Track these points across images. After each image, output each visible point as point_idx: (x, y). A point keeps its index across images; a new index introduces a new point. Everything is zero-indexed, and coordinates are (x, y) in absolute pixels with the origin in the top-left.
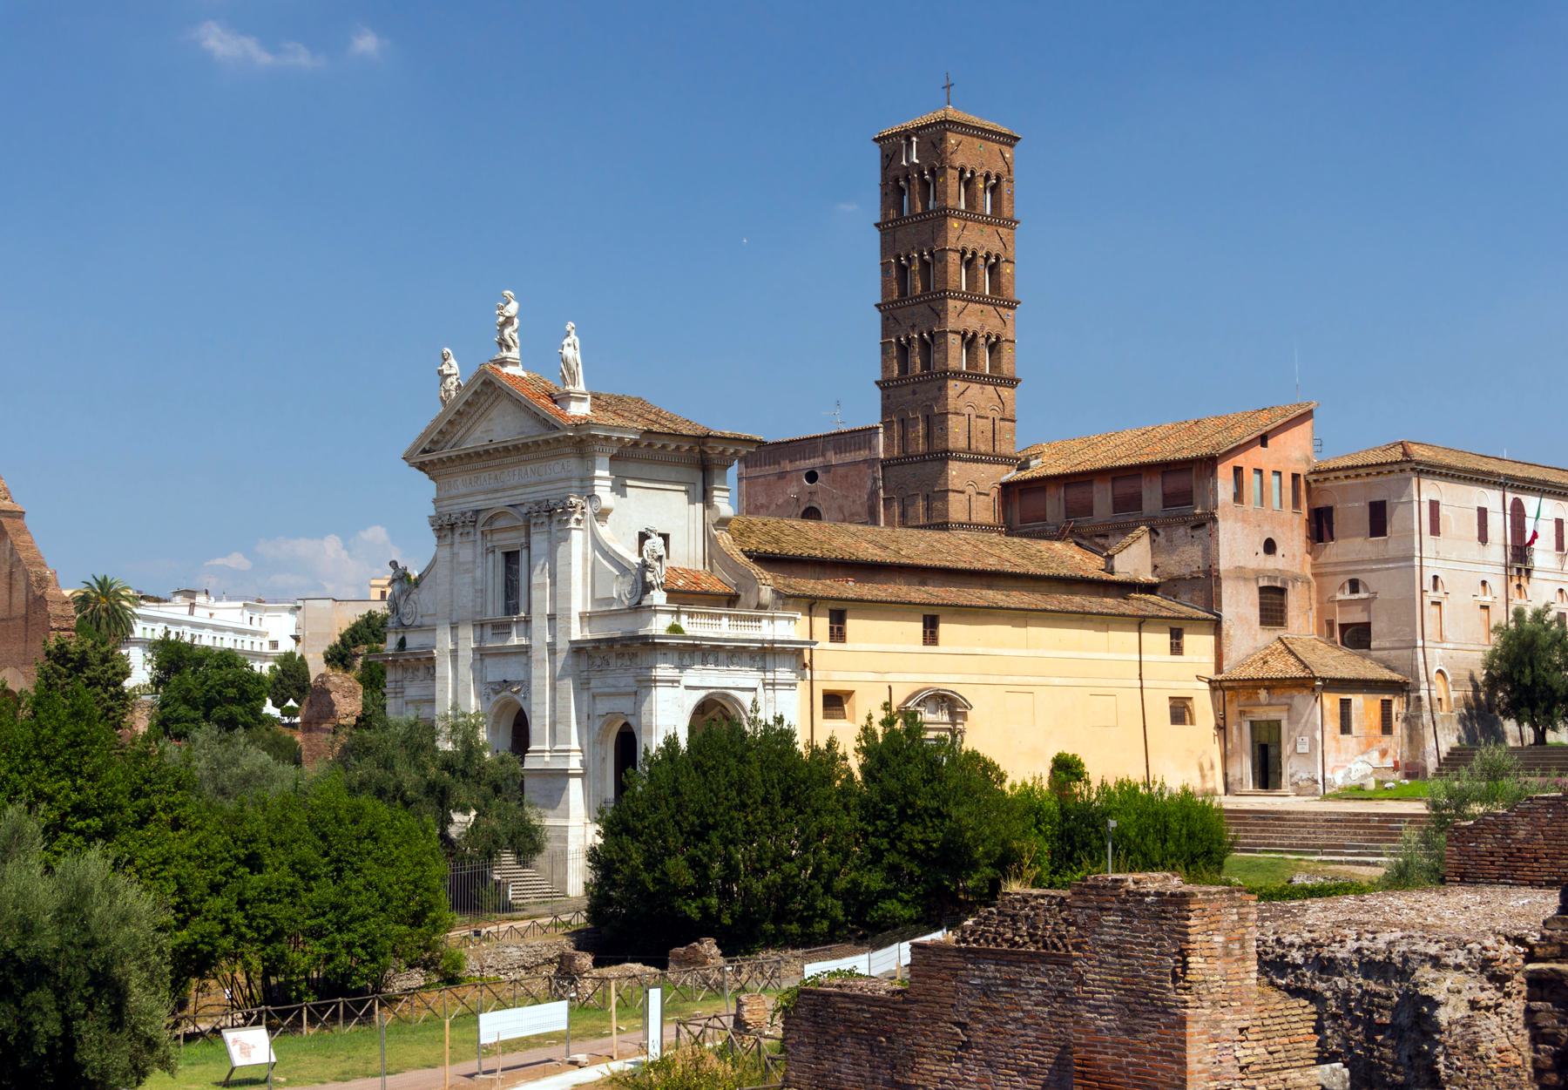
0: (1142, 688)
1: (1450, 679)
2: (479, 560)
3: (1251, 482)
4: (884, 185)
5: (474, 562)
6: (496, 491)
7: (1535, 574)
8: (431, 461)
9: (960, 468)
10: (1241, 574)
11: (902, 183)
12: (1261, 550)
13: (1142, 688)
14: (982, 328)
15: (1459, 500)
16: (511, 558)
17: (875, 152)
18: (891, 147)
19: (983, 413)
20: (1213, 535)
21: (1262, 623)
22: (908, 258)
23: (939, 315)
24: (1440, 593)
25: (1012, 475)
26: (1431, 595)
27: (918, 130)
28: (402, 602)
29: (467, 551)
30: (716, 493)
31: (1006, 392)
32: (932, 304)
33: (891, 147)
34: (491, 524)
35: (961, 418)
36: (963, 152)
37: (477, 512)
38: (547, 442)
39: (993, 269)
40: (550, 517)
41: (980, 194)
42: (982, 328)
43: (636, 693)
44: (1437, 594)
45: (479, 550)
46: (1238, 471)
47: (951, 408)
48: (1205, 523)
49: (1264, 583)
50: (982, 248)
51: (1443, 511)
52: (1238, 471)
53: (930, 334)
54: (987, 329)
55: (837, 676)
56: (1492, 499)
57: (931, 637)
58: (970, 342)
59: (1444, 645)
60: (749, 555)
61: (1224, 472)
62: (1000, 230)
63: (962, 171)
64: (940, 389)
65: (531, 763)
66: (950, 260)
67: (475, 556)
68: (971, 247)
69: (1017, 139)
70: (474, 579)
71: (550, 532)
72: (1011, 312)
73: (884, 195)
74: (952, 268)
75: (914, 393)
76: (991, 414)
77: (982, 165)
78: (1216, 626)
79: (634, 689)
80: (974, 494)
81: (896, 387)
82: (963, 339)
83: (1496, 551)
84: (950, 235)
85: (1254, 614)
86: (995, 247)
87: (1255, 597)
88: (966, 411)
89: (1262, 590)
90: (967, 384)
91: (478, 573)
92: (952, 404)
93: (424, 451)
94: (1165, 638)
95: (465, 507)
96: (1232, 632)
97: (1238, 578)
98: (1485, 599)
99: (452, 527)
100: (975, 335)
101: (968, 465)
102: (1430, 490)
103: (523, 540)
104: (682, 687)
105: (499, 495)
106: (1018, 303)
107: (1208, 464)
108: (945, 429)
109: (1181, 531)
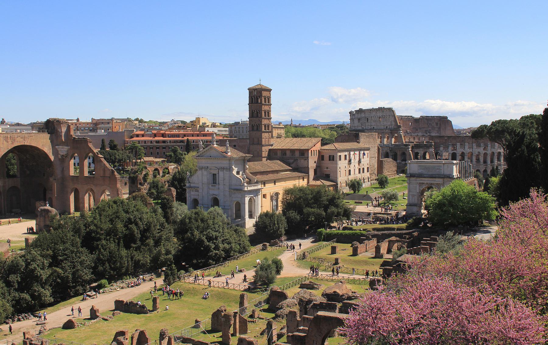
3: (313, 152)
15: (343, 154)
20: (308, 161)
22: (254, 111)
23: (261, 122)
25: (270, 148)
26: (339, 170)
36: (264, 94)
37: (208, 167)
39: (268, 113)
46: (311, 151)
48: (307, 159)
52: (311, 151)
53: (259, 124)
56: (347, 153)
57: (275, 184)
60: (251, 173)
61: (310, 151)
83: (347, 161)
91: (208, 176)
92: (263, 136)
102: (339, 154)
107: (308, 150)
108: (262, 141)
109: (302, 160)
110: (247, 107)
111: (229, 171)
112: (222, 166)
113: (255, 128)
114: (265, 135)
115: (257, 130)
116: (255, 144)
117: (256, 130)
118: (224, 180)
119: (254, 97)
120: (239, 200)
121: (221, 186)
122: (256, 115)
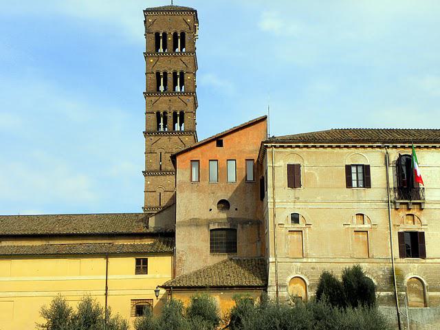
0: (106, 294)
1: (308, 284)
7: (425, 206)
9: (153, 180)
10: (195, 223)
12: (215, 208)
13: (106, 294)
14: (170, 108)
21: (212, 251)
24: (301, 225)
35: (154, 155)
42: (170, 108)
44: (297, 225)
49: (212, 227)
50: (170, 69)
51: (304, 171)
54: (173, 109)
59: (305, 260)
77: (170, 29)
78: (172, 253)
85: (207, 245)
86: (179, 67)
87: (206, 235)
89: (211, 230)
94: (131, 262)
96: (184, 258)
97: (190, 225)
98: (362, 226)
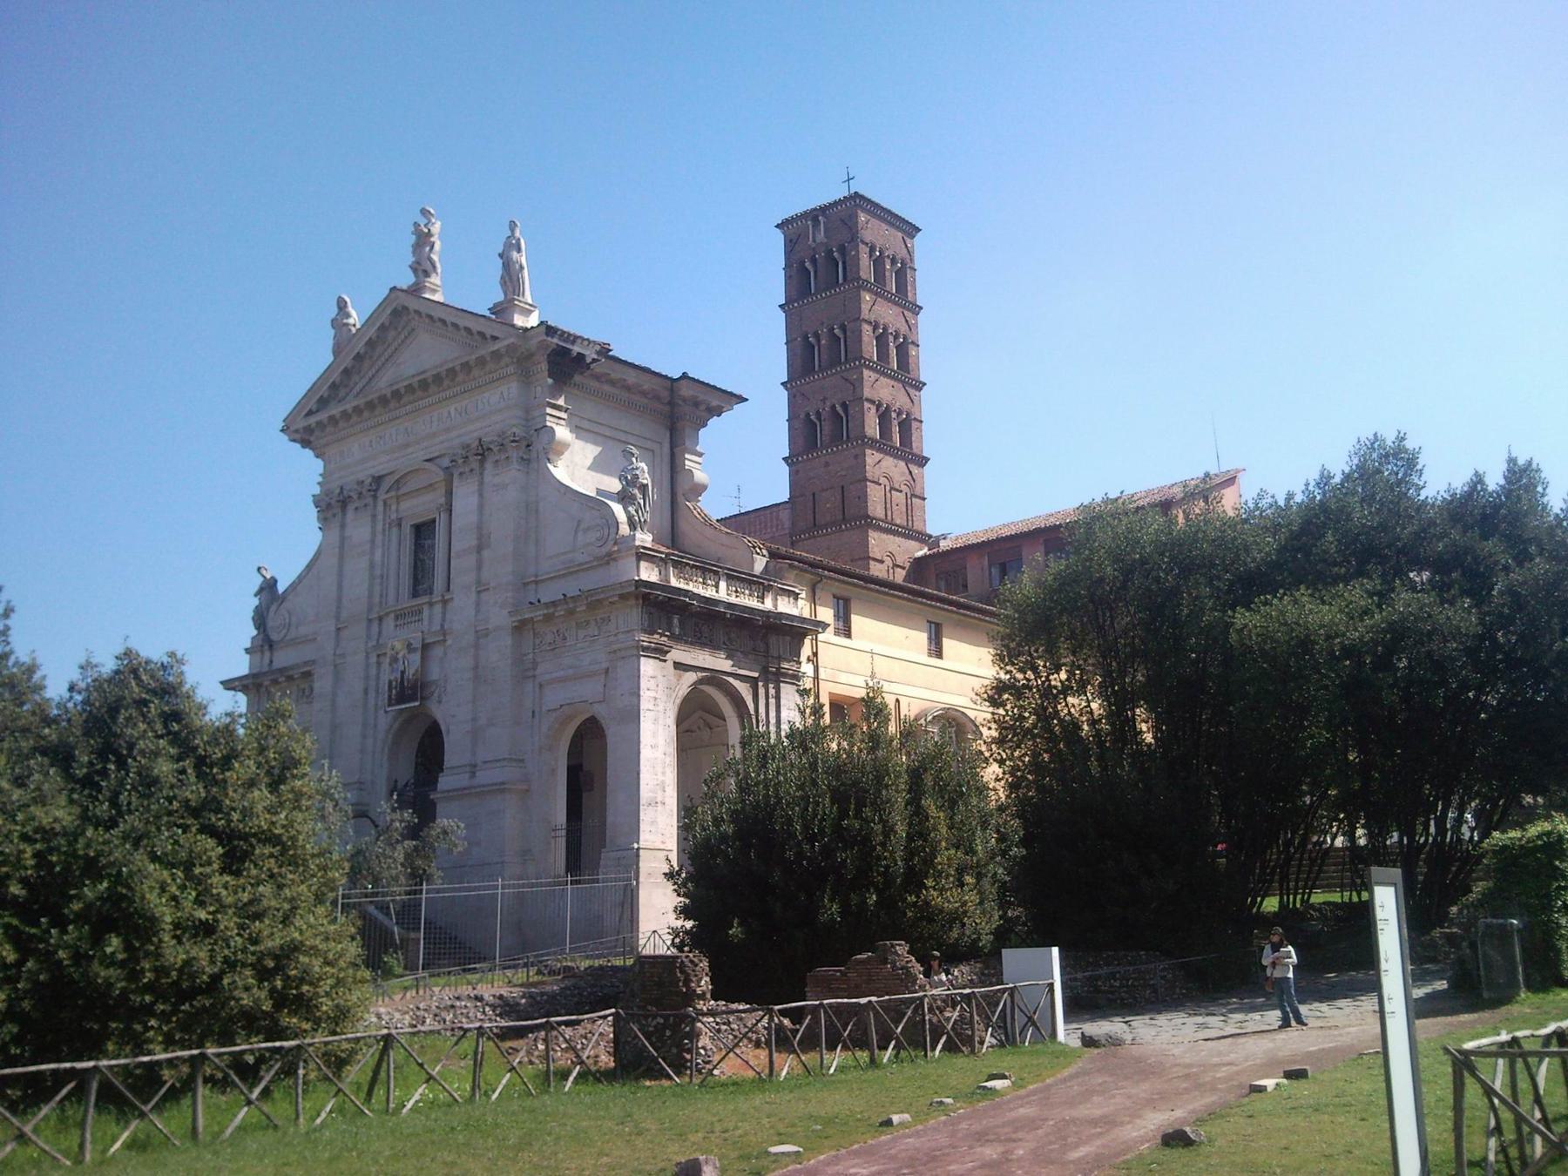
2: (379, 538)
4: (787, 267)
5: (373, 542)
6: (407, 445)
8: (319, 423)
11: (807, 264)
16: (423, 531)
17: (779, 238)
18: (795, 230)
19: (897, 487)
22: (817, 336)
27: (823, 209)
28: (271, 614)
29: (359, 529)
30: (687, 456)
31: (915, 469)
32: (845, 374)
33: (795, 230)
34: (398, 489)
37: (378, 480)
38: (481, 361)
40: (482, 462)
41: (887, 274)
43: (607, 671)
45: (379, 527)
47: (869, 475)
55: (843, 678)
58: (884, 417)
62: (906, 312)
63: (872, 249)
64: (856, 457)
65: (445, 782)
66: (864, 331)
67: (374, 533)
68: (882, 322)
69: (918, 230)
70: (372, 566)
71: (481, 483)
72: (917, 393)
73: (788, 278)
74: (865, 339)
75: (827, 464)
76: (903, 488)
79: (604, 665)
80: (891, 565)
81: (803, 461)
82: (877, 411)
84: (863, 306)
88: (883, 480)
90: (882, 455)
91: (378, 553)
92: (870, 472)
93: (310, 413)
95: (361, 477)
99: (344, 503)
100: (888, 407)
101: (884, 536)
103: (442, 500)
104: (670, 664)
105: (410, 450)
106: (924, 384)
108: (863, 497)
110: (777, 325)
111: (526, 461)
112: (471, 432)
113: (827, 427)
114: (880, 465)
115: (837, 438)
116: (826, 526)
117: (826, 439)
118: (479, 548)
119: (814, 261)
120: (588, 690)
121: (463, 605)
122: (825, 357)
